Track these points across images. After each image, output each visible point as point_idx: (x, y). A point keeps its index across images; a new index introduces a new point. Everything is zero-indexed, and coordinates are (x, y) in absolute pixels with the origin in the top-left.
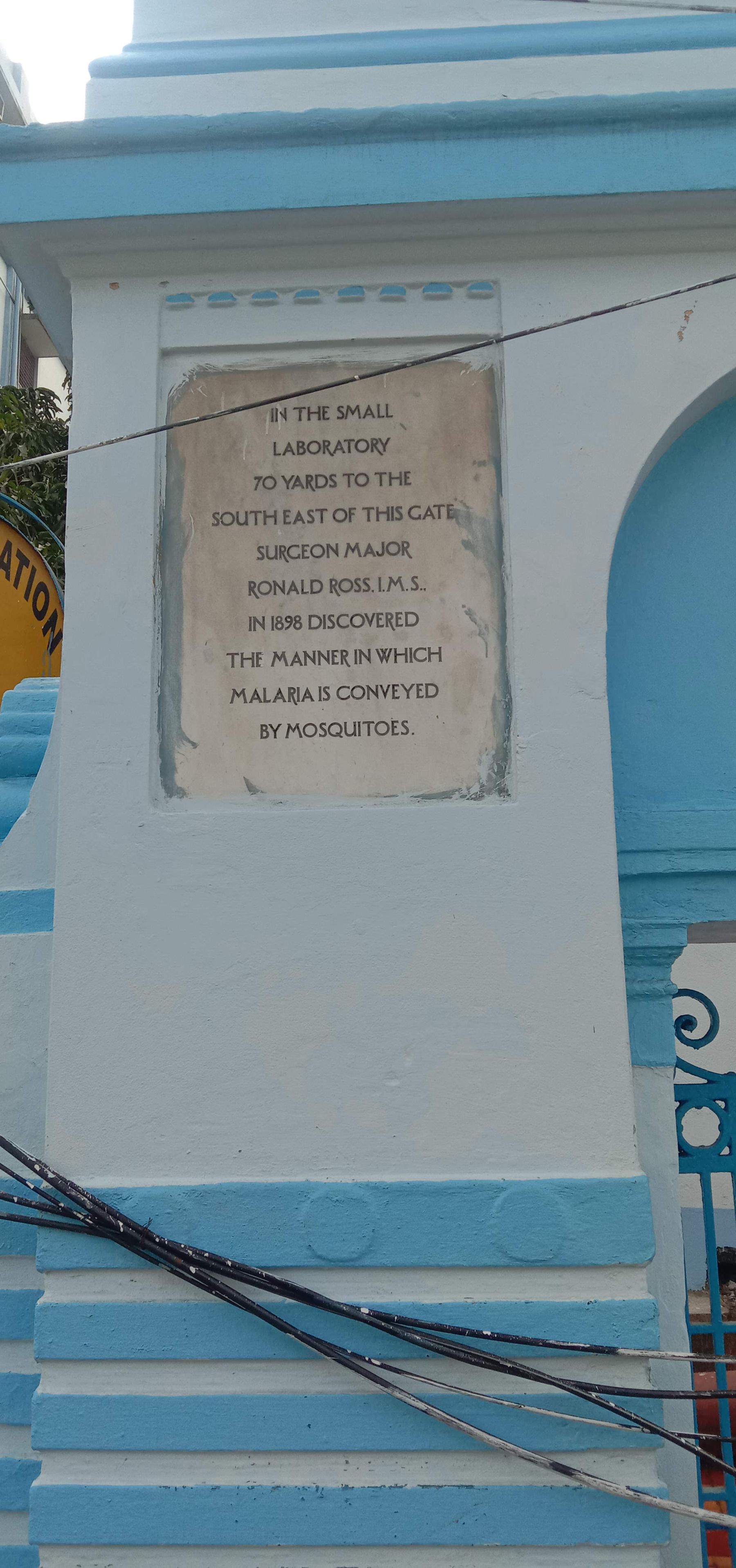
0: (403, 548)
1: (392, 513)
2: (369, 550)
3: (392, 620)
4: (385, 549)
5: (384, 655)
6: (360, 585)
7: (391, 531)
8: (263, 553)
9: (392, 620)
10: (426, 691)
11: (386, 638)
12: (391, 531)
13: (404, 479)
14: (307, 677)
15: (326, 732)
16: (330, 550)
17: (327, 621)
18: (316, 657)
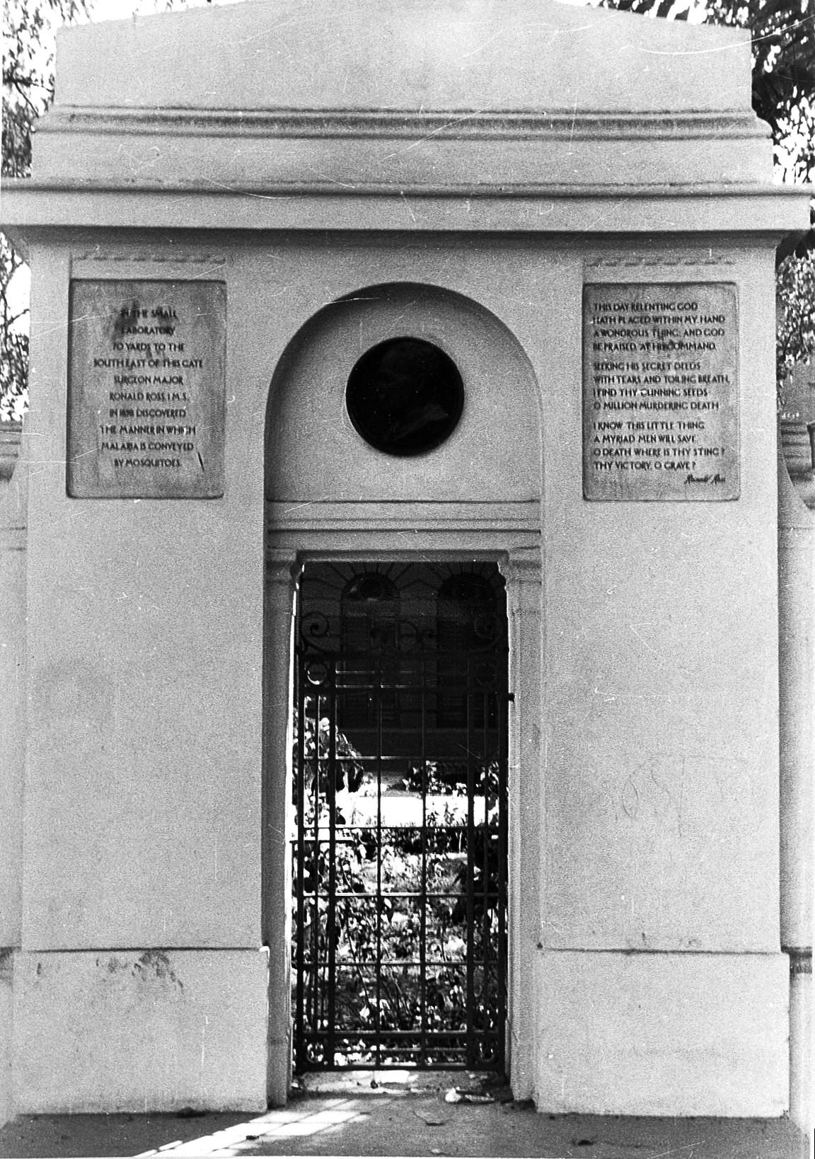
0: (180, 380)
1: (175, 364)
2: (165, 380)
3: (173, 414)
4: (171, 380)
5: (170, 430)
6: (160, 397)
7: (175, 373)
8: (116, 379)
9: (173, 414)
10: (188, 447)
11: (168, 422)
12: (175, 373)
13: (181, 347)
14: (137, 440)
15: (144, 464)
16: (147, 379)
17: (144, 413)
18: (140, 430)
